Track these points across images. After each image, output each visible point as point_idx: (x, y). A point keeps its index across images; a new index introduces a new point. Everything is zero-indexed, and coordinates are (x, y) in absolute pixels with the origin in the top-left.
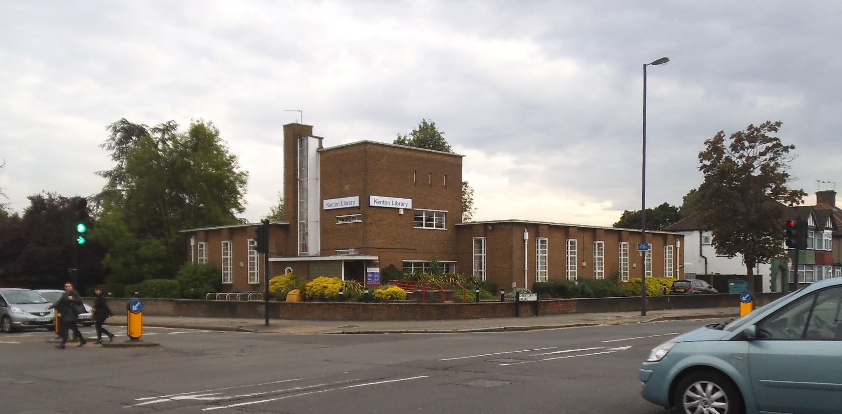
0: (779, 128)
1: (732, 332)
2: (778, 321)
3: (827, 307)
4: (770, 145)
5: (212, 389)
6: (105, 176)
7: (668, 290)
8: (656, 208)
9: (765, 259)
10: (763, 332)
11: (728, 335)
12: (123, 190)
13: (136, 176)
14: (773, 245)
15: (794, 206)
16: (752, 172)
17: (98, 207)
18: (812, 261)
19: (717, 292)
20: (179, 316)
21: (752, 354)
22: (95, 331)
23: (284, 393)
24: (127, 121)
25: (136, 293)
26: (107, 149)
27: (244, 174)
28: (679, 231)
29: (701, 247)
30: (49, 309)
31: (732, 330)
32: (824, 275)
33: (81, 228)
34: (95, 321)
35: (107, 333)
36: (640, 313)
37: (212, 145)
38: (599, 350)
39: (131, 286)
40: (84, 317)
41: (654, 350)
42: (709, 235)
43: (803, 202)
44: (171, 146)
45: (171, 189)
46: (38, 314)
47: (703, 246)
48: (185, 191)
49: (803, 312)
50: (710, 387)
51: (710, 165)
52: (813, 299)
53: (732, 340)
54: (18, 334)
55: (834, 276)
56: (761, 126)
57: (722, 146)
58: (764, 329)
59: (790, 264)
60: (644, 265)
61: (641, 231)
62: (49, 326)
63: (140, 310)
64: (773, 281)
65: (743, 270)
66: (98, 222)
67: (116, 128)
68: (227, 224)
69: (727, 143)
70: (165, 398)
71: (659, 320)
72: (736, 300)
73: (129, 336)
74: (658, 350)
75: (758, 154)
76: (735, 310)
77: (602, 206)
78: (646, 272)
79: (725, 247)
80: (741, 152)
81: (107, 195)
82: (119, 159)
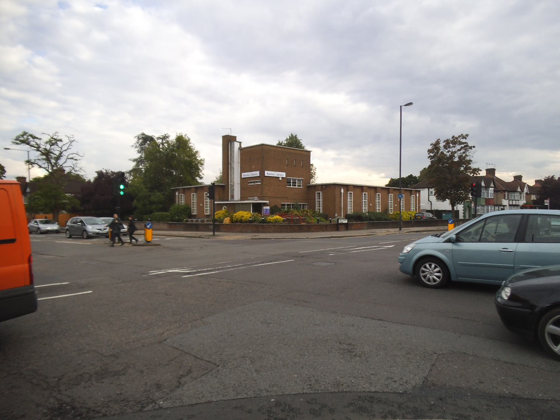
0: (467, 137)
1: (444, 238)
2: (467, 233)
3: (491, 226)
4: (463, 146)
5: (187, 266)
6: (134, 161)
7: (412, 218)
8: (406, 177)
9: (460, 202)
10: (459, 239)
11: (442, 240)
12: (143, 168)
13: (149, 161)
14: (464, 195)
15: (475, 176)
16: (454, 159)
17: (130, 177)
18: (484, 203)
19: (436, 218)
20: (170, 230)
21: (454, 249)
22: (129, 238)
23: (222, 269)
24: (145, 134)
25: (149, 219)
26: (135, 148)
27: (203, 160)
28: (418, 188)
29: (429, 196)
30: (106, 227)
31: (444, 237)
32: (489, 210)
33: (122, 187)
34: (129, 233)
35: (134, 239)
36: (398, 229)
37: (187, 146)
38: (378, 247)
39: (146, 216)
40: (123, 231)
41: (405, 247)
42: (433, 190)
43: (479, 174)
44: (166, 146)
45: (166, 167)
46: (100, 230)
47: (429, 196)
48: (173, 168)
49: (479, 229)
50: (433, 266)
51: (433, 156)
52: (484, 222)
53: (444, 242)
54: (89, 239)
55: (494, 211)
56: (459, 136)
57: (439, 146)
58: (460, 237)
59: (473, 205)
60: (401, 205)
61: (399, 188)
62: (106, 235)
63: (151, 228)
64: (464, 213)
65: (449, 208)
66: (130, 184)
67: (139, 137)
68: (194, 185)
69: (442, 145)
70: (163, 271)
71: (408, 232)
72: (446, 223)
73: (146, 240)
74: (407, 247)
75: (457, 150)
76: (446, 228)
77: (380, 176)
78: (401, 208)
79: (441, 196)
80: (449, 149)
81: (135, 171)
82: (141, 153)
